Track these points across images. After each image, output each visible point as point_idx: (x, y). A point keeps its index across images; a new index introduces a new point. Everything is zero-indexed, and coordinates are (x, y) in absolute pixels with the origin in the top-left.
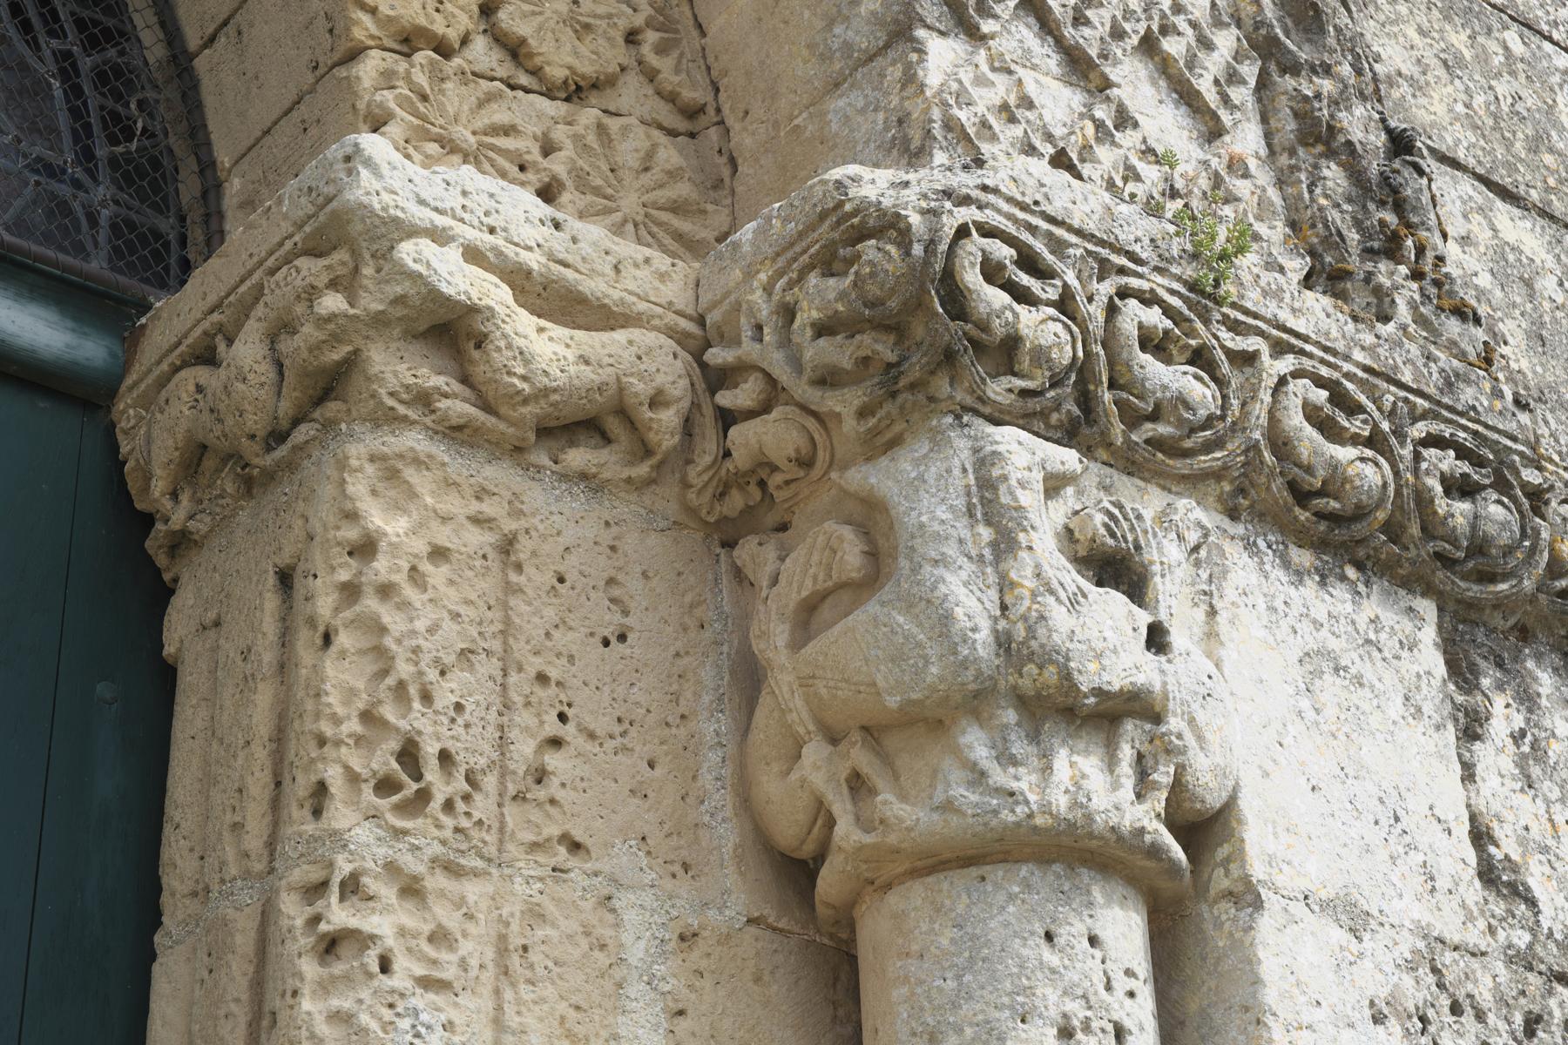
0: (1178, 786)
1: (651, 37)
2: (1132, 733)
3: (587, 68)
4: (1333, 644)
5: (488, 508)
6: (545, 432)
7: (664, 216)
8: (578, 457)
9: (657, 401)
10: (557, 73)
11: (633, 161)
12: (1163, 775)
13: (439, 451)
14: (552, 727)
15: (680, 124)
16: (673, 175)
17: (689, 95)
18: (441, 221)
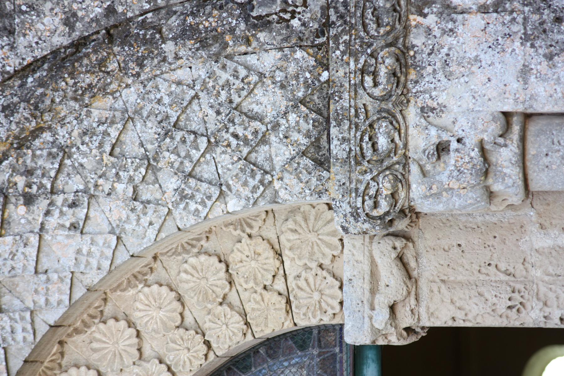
0: (501, 136)
1: (248, 230)
2: (487, 147)
3: (271, 254)
4: (438, 65)
5: (435, 290)
6: (410, 278)
7: (311, 225)
8: (412, 264)
9: (395, 248)
10: (278, 263)
11: (296, 236)
12: (501, 141)
13: (423, 304)
14: (492, 269)
15: (271, 215)
16: (295, 222)
17: (263, 216)
18: (367, 320)
